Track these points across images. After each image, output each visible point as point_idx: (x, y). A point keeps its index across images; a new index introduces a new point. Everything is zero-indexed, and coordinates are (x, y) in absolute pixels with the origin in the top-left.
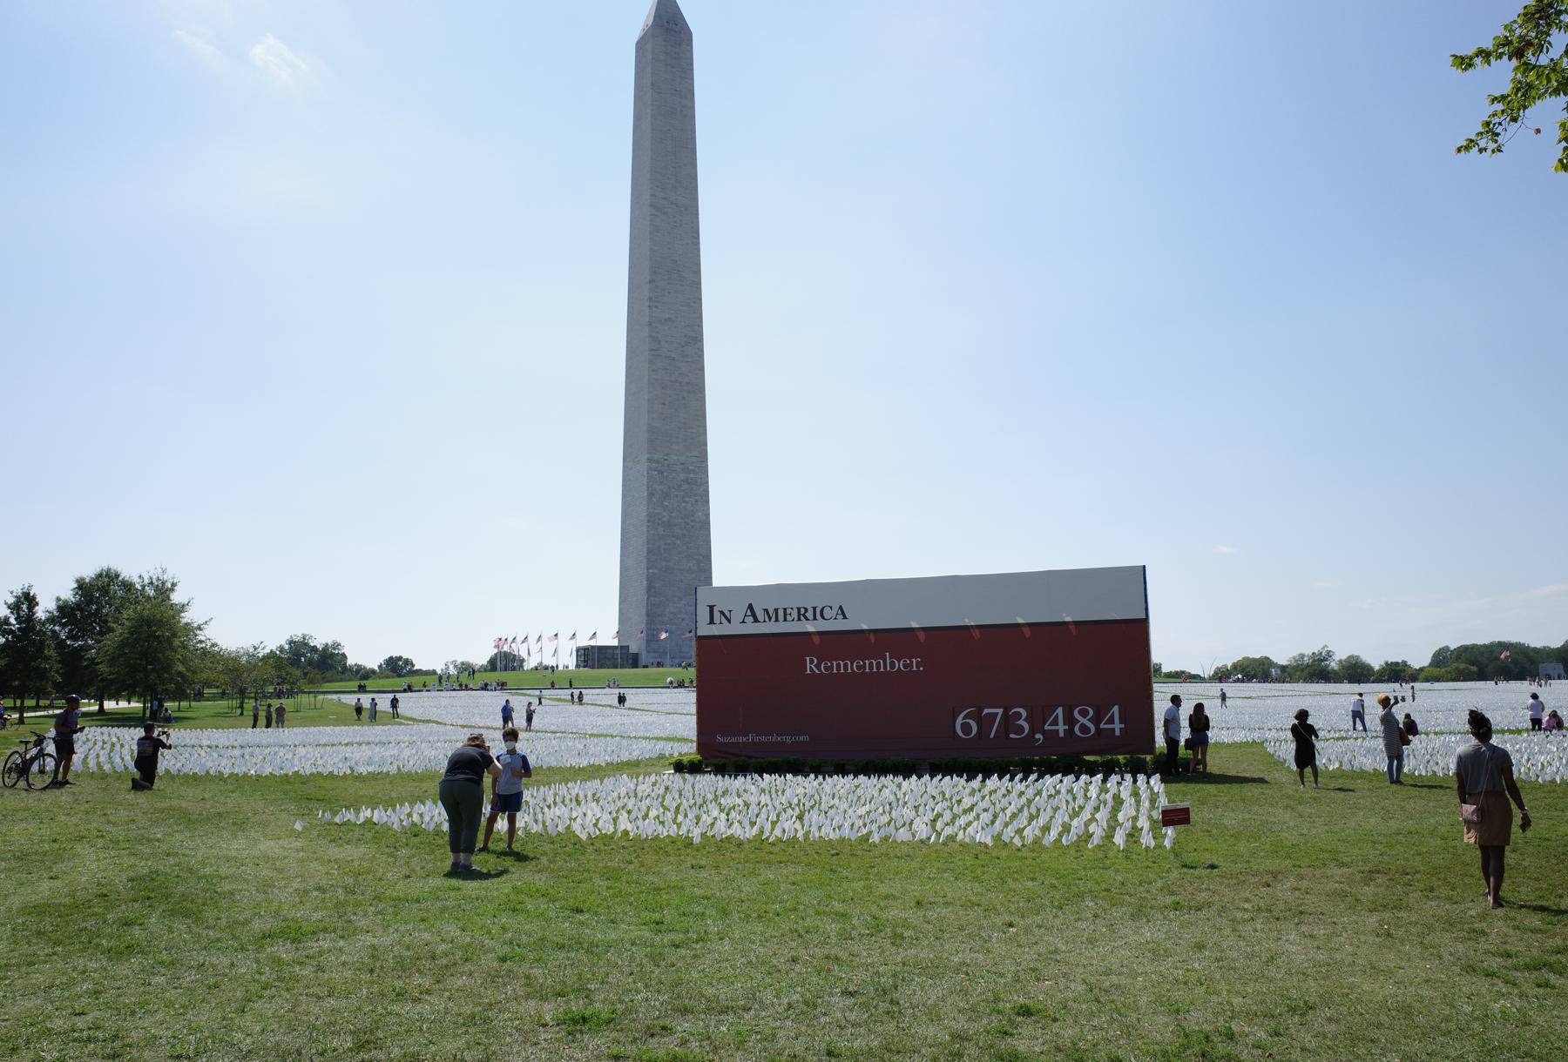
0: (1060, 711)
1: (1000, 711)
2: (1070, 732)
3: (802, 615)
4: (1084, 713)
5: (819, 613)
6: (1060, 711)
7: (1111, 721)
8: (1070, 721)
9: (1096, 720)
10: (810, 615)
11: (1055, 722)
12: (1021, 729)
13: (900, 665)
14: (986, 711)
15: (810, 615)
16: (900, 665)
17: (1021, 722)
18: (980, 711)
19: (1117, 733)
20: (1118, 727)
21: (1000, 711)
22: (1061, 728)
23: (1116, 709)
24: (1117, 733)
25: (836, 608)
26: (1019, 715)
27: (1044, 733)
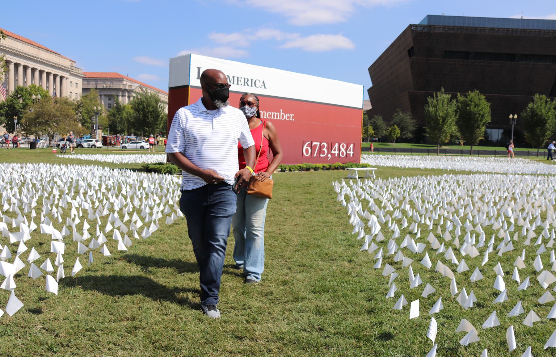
0: (337, 145)
1: (318, 144)
2: (339, 154)
3: (245, 83)
4: (343, 146)
5: (254, 83)
6: (337, 145)
7: (350, 151)
8: (339, 150)
9: (346, 150)
10: (249, 83)
11: (335, 150)
12: (324, 152)
13: (285, 117)
14: (314, 143)
15: (249, 83)
16: (285, 117)
17: (325, 149)
18: (312, 143)
19: (351, 156)
20: (352, 153)
21: (318, 144)
22: (337, 152)
23: (352, 146)
24: (351, 156)
25: (261, 82)
26: (324, 146)
27: (331, 154)
